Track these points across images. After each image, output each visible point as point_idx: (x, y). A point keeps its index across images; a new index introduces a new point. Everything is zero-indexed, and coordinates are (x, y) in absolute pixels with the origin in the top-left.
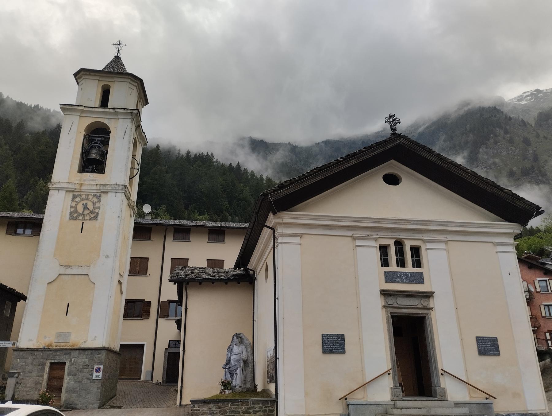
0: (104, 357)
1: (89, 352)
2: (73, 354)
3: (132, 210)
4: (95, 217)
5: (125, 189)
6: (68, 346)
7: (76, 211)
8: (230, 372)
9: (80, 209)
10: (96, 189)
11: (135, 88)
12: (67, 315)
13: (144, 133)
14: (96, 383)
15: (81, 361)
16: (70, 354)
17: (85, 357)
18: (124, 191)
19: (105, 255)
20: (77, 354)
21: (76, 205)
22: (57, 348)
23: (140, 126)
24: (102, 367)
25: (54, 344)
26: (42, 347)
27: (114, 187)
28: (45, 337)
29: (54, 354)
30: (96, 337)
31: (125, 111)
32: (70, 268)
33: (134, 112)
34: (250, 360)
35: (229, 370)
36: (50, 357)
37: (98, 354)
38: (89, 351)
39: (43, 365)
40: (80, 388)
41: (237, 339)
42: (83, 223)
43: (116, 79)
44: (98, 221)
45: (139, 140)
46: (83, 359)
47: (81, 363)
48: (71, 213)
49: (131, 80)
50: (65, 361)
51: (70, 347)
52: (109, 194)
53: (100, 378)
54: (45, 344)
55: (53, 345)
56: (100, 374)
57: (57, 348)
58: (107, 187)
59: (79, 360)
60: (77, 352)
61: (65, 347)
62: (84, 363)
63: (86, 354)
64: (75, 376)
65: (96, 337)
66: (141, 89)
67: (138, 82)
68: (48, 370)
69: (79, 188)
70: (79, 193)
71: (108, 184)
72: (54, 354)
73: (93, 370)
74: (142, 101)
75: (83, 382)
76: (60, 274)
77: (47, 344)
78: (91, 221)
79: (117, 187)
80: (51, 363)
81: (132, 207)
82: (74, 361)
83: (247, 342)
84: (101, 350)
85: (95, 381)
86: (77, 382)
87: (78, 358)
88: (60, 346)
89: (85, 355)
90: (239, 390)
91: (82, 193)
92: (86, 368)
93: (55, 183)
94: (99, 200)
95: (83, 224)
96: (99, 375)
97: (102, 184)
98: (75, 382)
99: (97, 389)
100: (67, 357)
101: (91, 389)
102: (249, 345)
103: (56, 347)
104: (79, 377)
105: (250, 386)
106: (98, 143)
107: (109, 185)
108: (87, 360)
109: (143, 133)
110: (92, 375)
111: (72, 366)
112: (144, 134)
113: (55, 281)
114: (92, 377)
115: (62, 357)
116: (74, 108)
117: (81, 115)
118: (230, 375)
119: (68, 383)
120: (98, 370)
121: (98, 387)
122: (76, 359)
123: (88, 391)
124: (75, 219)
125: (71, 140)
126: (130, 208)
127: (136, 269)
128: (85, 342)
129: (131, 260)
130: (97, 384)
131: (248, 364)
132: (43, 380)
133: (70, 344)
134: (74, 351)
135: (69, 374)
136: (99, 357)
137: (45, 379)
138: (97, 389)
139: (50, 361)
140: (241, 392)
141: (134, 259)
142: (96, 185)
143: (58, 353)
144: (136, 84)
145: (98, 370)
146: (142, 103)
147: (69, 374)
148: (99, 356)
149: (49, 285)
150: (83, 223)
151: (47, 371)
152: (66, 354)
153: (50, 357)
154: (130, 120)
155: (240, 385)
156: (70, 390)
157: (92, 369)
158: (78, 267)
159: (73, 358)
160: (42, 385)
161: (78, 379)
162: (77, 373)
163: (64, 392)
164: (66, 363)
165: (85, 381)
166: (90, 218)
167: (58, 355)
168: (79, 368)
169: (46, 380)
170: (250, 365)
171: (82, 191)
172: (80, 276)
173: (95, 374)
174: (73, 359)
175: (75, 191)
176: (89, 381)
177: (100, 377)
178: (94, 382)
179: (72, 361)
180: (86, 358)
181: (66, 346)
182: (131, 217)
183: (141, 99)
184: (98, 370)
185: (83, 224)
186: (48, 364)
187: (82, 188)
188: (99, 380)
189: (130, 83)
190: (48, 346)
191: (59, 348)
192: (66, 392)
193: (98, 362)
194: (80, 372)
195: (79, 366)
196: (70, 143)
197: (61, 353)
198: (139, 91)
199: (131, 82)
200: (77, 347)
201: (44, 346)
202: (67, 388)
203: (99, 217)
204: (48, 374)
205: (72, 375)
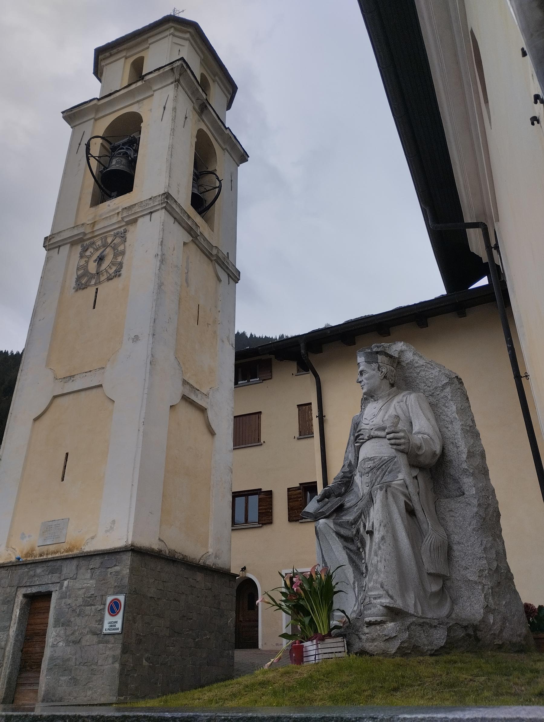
0: (128, 571)
1: (96, 562)
2: (69, 568)
3: (216, 265)
4: (116, 271)
5: (166, 200)
6: (62, 550)
7: (86, 273)
8: (343, 531)
9: (92, 267)
10: (117, 221)
11: (187, 43)
12: (63, 480)
13: (228, 128)
14: (110, 646)
15: (80, 587)
16: (59, 570)
17: (88, 576)
18: (164, 205)
19: (133, 337)
20: (74, 568)
21: (87, 262)
22: (41, 558)
23: (206, 106)
24: (122, 598)
25: (37, 551)
26: (13, 559)
27: (147, 204)
28: (23, 536)
29: (32, 573)
30: (114, 522)
31: (161, 71)
32: (71, 381)
33: (175, 65)
34: (464, 456)
35: (335, 524)
36: (24, 581)
37: (115, 566)
38: (98, 558)
39: (10, 602)
40: (76, 659)
41: (374, 366)
42: (97, 289)
43: (150, 41)
44: (121, 277)
45: (222, 145)
46: (85, 581)
47: (81, 592)
48: (79, 278)
49: (176, 29)
50: (51, 588)
51: (66, 554)
52: (140, 221)
53: (118, 629)
54: (22, 552)
55: (34, 552)
56: (119, 619)
57: (41, 558)
58: (134, 210)
59: (77, 585)
60: (75, 562)
61: (57, 555)
62: (88, 589)
63: (91, 567)
64: (68, 625)
65: (114, 522)
66: (204, 49)
67: (190, 30)
68: (18, 613)
69: (91, 231)
70: (92, 240)
71: (135, 204)
72: (32, 573)
73: (104, 609)
74: (218, 80)
75: (84, 643)
76: (55, 397)
77: (25, 552)
78: (110, 281)
79: (151, 202)
80: (25, 596)
81: (215, 258)
82: (67, 587)
83: (435, 372)
84: (121, 554)
85: (107, 638)
86: (71, 644)
87: (75, 579)
88: (47, 554)
89: (89, 571)
90: (389, 639)
91: (95, 239)
92: (91, 605)
93: (53, 236)
94: (122, 239)
95: (96, 292)
96: (116, 622)
97: (126, 208)
98: (68, 643)
99: (113, 663)
100: (55, 578)
101: (100, 662)
102: (444, 387)
103: (41, 555)
104: (76, 628)
105: (487, 609)
106: (123, 149)
107: (137, 205)
108: (92, 582)
109: (226, 128)
110: (101, 621)
111: (64, 601)
112: (228, 130)
113: (48, 413)
114: (102, 627)
115: (47, 579)
116: (82, 108)
117: (97, 117)
118: (345, 548)
119: (53, 646)
120: (115, 608)
121: (114, 656)
122: (72, 582)
123: (93, 667)
124: (83, 286)
125: (80, 161)
126: (212, 261)
127: (309, 425)
128: (93, 538)
129: (299, 410)
130: (112, 647)
131: (456, 481)
132: (7, 641)
133: (65, 546)
134: (68, 561)
135: (57, 623)
136: (117, 573)
137: (11, 637)
138: (113, 663)
139: (23, 591)
140: (402, 652)
141: (304, 407)
142: (116, 215)
143: (39, 571)
144: (187, 36)
145: (114, 609)
146: (220, 83)
147: (57, 623)
148: (117, 568)
149: (37, 422)
150: (97, 289)
151: (16, 615)
152: (52, 572)
153: (24, 581)
154: (173, 85)
155: (386, 601)
156: (55, 665)
157: (102, 607)
158: (84, 374)
159: (65, 580)
160: (5, 649)
161: (73, 634)
162: (72, 619)
163: (45, 673)
164: (53, 594)
165: (87, 641)
166: (109, 275)
167: (39, 576)
168: (76, 605)
169: (13, 638)
170: (465, 487)
171: (96, 233)
172: (88, 392)
173: (108, 619)
174: (66, 583)
175: (85, 238)
176: (95, 639)
177: (119, 625)
178: (107, 642)
179: (64, 588)
180: (91, 578)
181: (57, 552)
182: (220, 280)
183: (215, 76)
184: (115, 608)
185: (96, 292)
186: (20, 599)
187: (95, 229)
188: (116, 636)
189: (174, 36)
190: (28, 555)
191: (45, 557)
192: (49, 670)
193: (116, 584)
194: (79, 615)
195: (77, 600)
196: (79, 165)
197: (43, 569)
198: (201, 54)
199: (177, 34)
200: (76, 552)
201: (18, 556)
202: (52, 659)
203: (123, 272)
204: (18, 623)
205: (63, 625)
